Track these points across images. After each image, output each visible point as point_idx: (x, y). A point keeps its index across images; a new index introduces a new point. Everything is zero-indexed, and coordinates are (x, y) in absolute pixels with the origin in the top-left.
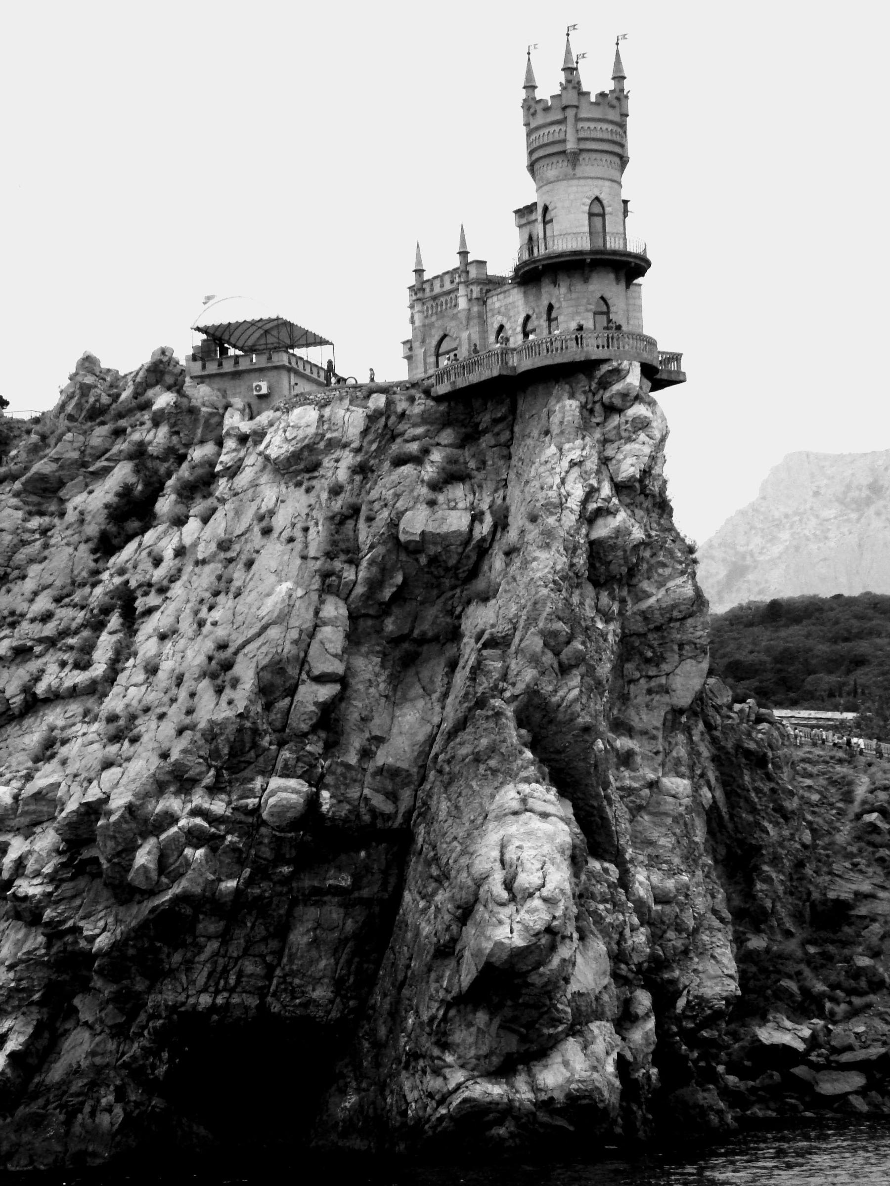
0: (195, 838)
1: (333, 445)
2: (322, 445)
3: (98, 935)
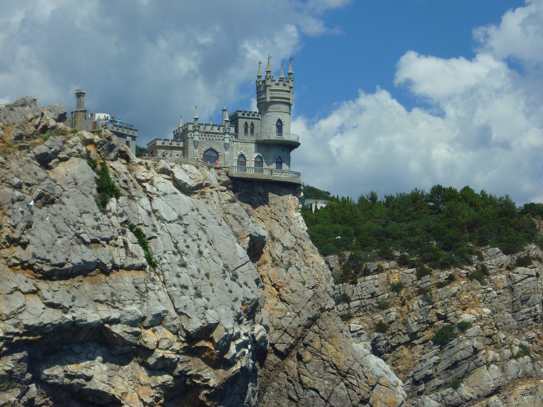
0: (245, 344)
1: (207, 185)
2: (204, 184)
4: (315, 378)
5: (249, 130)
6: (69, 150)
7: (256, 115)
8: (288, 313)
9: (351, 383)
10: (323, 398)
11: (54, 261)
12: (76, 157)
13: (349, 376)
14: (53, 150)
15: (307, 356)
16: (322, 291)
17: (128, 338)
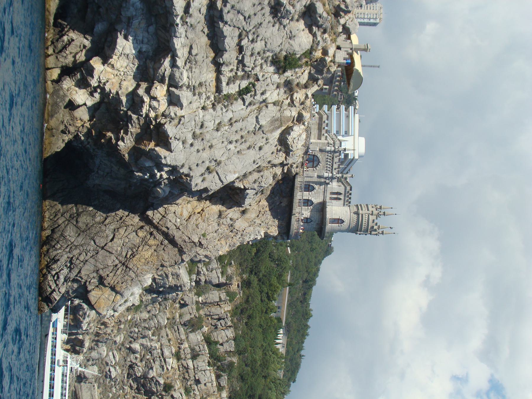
3: (124, 143)
4: (123, 239)
5: (335, 196)
6: (319, 34)
7: (347, 203)
8: (179, 220)
9: (118, 269)
10: (105, 245)
11: (225, 10)
12: (313, 40)
13: (124, 268)
14: (319, 19)
15: (141, 234)
16: (197, 250)
17: (161, 71)
